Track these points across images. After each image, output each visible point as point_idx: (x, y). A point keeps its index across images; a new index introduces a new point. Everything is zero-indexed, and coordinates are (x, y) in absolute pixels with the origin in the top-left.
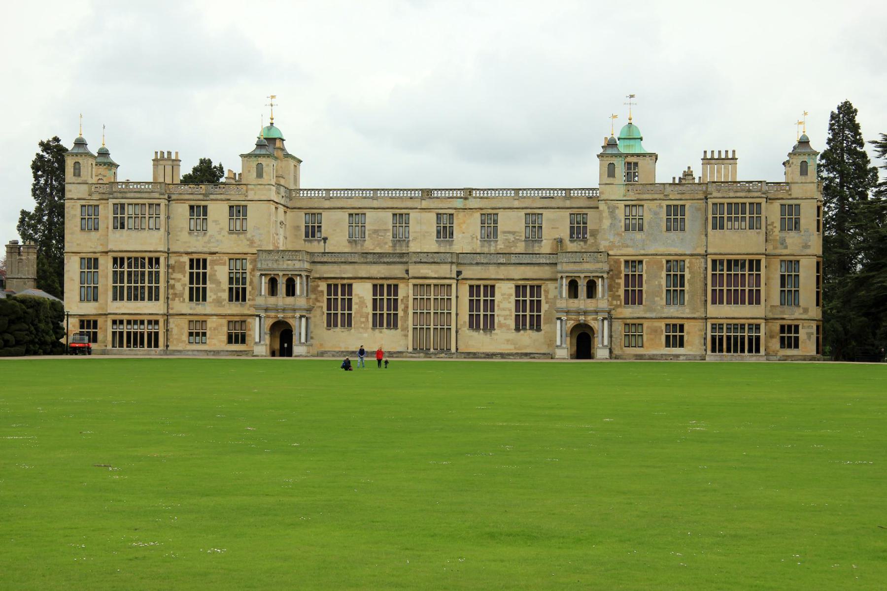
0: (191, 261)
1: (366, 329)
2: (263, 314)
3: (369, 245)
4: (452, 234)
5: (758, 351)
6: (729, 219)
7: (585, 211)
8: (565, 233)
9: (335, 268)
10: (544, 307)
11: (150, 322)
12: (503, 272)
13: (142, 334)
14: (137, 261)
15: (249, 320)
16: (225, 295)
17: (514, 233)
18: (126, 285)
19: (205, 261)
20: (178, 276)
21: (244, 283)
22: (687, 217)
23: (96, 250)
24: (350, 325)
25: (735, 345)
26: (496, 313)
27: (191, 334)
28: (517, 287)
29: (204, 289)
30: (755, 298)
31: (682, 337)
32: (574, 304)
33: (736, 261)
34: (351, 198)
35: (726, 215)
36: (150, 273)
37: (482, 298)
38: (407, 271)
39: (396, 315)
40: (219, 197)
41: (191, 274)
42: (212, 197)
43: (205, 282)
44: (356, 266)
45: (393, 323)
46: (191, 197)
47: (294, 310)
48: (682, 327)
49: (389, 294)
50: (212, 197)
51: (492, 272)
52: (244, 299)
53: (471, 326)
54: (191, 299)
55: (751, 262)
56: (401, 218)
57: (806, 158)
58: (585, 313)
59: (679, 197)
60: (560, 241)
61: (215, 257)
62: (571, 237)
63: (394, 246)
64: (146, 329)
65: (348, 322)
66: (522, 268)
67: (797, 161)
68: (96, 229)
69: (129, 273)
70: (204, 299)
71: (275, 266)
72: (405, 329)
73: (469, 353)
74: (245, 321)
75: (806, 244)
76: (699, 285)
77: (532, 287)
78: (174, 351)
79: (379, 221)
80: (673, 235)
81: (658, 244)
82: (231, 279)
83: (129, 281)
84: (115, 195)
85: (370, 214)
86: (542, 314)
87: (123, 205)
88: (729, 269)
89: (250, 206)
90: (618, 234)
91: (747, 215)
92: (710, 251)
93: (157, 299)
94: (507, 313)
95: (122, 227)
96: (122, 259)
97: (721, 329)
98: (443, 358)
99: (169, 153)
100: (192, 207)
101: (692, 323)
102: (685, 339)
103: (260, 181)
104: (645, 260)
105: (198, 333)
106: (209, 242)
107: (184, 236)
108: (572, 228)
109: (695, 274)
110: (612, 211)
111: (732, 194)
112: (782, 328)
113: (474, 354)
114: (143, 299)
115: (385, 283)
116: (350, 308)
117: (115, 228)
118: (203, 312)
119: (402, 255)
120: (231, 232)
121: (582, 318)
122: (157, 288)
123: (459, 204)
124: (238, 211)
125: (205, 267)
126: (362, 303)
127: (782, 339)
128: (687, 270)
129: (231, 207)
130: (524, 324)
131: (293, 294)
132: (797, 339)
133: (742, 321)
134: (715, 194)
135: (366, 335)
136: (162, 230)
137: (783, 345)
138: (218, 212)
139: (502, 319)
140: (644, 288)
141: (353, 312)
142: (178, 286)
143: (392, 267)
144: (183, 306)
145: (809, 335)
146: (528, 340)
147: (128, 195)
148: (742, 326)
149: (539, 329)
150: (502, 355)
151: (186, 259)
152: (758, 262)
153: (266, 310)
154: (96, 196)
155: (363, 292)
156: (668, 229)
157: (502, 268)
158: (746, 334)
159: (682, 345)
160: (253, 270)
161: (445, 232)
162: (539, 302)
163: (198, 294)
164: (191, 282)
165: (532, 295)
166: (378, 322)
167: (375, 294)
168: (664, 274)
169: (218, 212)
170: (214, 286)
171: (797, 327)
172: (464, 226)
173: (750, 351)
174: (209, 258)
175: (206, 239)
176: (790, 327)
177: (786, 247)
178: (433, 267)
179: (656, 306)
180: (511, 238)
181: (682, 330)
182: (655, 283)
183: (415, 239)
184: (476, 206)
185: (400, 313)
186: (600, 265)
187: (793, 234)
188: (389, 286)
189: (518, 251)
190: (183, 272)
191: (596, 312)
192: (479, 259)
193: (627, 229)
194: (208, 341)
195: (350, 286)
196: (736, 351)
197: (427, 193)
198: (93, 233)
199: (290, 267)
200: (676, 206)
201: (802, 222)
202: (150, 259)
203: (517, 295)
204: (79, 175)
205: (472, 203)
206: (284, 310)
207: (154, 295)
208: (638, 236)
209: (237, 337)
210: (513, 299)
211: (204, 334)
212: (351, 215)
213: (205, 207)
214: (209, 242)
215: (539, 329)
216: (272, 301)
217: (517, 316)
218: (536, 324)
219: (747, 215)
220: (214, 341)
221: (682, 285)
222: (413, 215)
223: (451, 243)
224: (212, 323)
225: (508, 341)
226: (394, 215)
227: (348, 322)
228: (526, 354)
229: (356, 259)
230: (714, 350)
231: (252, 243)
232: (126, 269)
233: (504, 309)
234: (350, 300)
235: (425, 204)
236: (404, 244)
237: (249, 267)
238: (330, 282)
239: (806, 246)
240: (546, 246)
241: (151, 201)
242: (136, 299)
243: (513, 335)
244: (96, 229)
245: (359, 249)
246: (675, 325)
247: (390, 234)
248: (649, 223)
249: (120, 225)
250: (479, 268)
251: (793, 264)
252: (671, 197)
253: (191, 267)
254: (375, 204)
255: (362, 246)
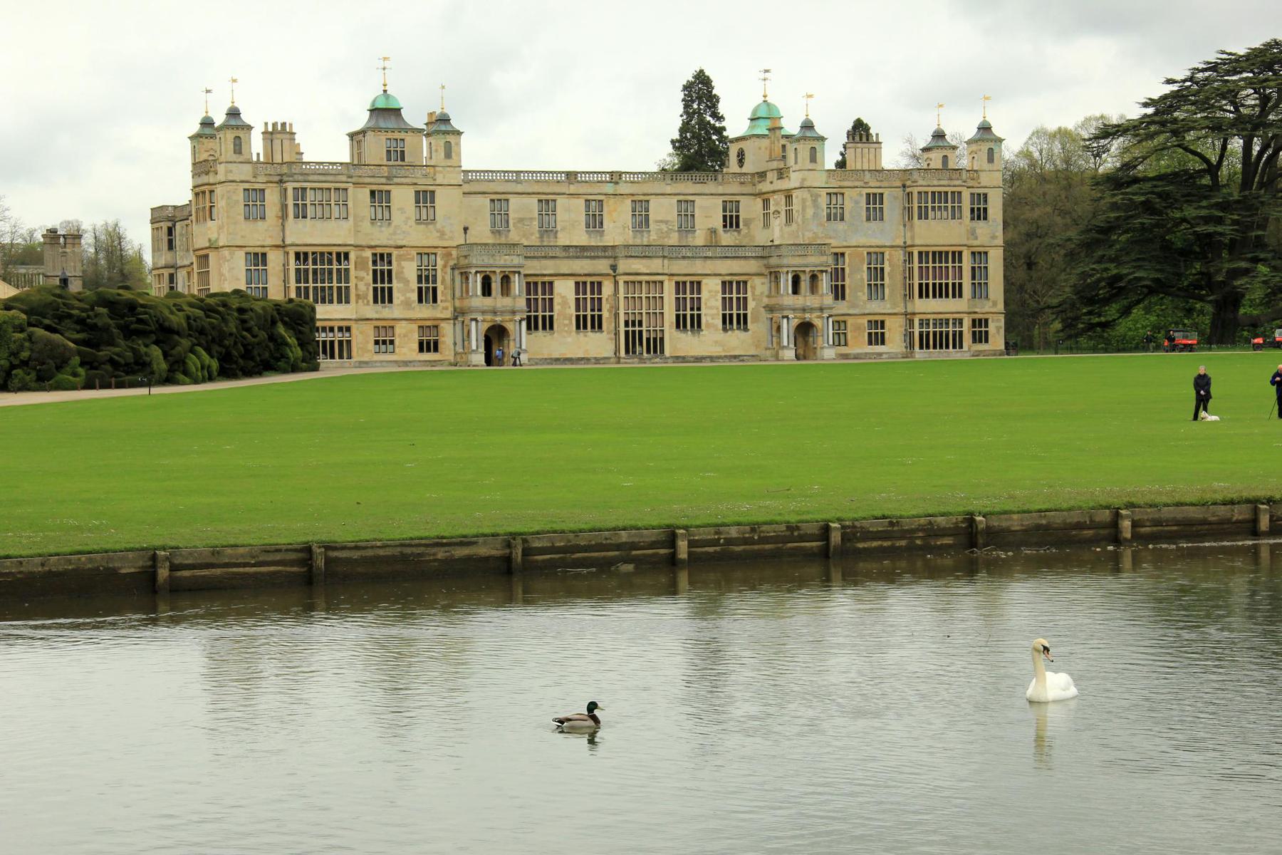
0: (374, 255)
1: (569, 332)
2: (480, 318)
3: (514, 236)
4: (602, 223)
5: (961, 347)
6: (933, 208)
7: (737, 198)
8: (718, 223)
9: (535, 263)
10: (751, 305)
11: (340, 329)
12: (710, 266)
13: (332, 343)
14: (321, 257)
15: (443, 325)
16: (415, 296)
17: (666, 222)
18: (311, 285)
19: (390, 255)
20: (362, 274)
21: (435, 281)
22: (885, 206)
23: (266, 243)
24: (551, 327)
25: (941, 341)
26: (703, 312)
27: (377, 342)
28: (724, 283)
29: (390, 289)
30: (957, 291)
31: (883, 334)
32: (799, 301)
33: (940, 253)
34: (493, 181)
35: (930, 205)
36: (338, 270)
37: (688, 296)
38: (614, 268)
39: (600, 317)
40: (403, 180)
41: (375, 272)
42: (396, 180)
43: (390, 281)
44: (558, 262)
45: (597, 324)
46: (372, 180)
47: (514, 312)
48: (883, 322)
49: (593, 293)
50: (396, 180)
51: (698, 267)
52: (435, 300)
53: (678, 326)
54: (375, 301)
55: (954, 253)
56: (547, 204)
57: (992, 145)
58: (812, 310)
59: (878, 184)
60: (713, 232)
61: (402, 251)
62: (725, 226)
63: (541, 237)
64: (338, 336)
65: (549, 324)
66: (729, 262)
67: (985, 147)
68: (263, 218)
69: (315, 271)
70: (390, 301)
71: (491, 262)
72: (617, 334)
73: (677, 357)
74: (436, 327)
75: (991, 234)
76: (899, 278)
77: (738, 283)
78: (360, 362)
79: (522, 208)
80: (873, 224)
81: (859, 235)
82: (420, 277)
83: (315, 281)
84: (296, 177)
85: (514, 200)
86: (749, 312)
87: (304, 189)
88: (934, 262)
89: (439, 192)
90: (821, 225)
91: (949, 205)
92: (917, 242)
93: (348, 302)
94: (714, 311)
95: (305, 217)
96: (306, 254)
97: (928, 324)
98: (657, 363)
99: (284, 125)
100: (372, 193)
101: (893, 319)
102: (886, 336)
103: (449, 162)
104: (847, 252)
105: (384, 342)
106: (395, 233)
107: (366, 225)
108: (725, 217)
109: (893, 265)
110: (815, 199)
111: (936, 183)
112: (974, 321)
113: (684, 358)
114: (331, 302)
115: (589, 280)
116: (551, 310)
117: (296, 217)
118: (391, 316)
119: (605, 248)
120: (419, 221)
121: (807, 315)
122: (347, 288)
123: (609, 188)
124: (425, 198)
125: (390, 263)
126: (565, 303)
127: (974, 333)
128: (887, 263)
129: (417, 193)
130: (731, 322)
131: (489, 294)
132: (987, 332)
133: (947, 316)
134: (921, 182)
135: (569, 340)
136: (351, 218)
137: (974, 341)
138: (403, 198)
139: (709, 318)
140: (847, 282)
141: (555, 314)
142: (362, 287)
143: (596, 262)
144: (372, 311)
145: (998, 328)
146: (737, 341)
147: (311, 178)
148: (947, 320)
149: (746, 329)
150: (712, 359)
151: (368, 254)
152: (960, 253)
153: (483, 312)
154: (260, 179)
155: (565, 291)
156: (868, 219)
157: (709, 262)
158: (951, 329)
159: (883, 343)
160: (445, 266)
161: (595, 222)
162: (745, 299)
163: (383, 296)
164: (375, 281)
165: (738, 292)
166: (581, 323)
167: (577, 293)
168: (865, 266)
169: (403, 198)
170: (401, 285)
171: (986, 321)
172: (615, 214)
173: (954, 347)
174: (395, 253)
175: (391, 230)
176: (980, 320)
177: (976, 238)
178: (644, 261)
179: (859, 303)
180: (664, 227)
181: (883, 327)
182: (856, 278)
183: (564, 229)
184: (627, 191)
185: (605, 314)
186: (824, 259)
187: (982, 223)
188: (592, 283)
189: (671, 242)
190: (364, 268)
191: (821, 309)
192: (684, 252)
193: (829, 219)
194: (397, 350)
195: (551, 283)
196: (941, 347)
197: (571, 176)
198: (260, 223)
199: (508, 263)
200: (875, 194)
201: (990, 212)
202: (338, 254)
203: (724, 292)
204: (240, 153)
205: (623, 188)
206: (502, 313)
207: (343, 297)
208: (840, 226)
209: (429, 345)
210: (720, 296)
211: (392, 342)
212: (492, 201)
213: (388, 192)
214: (395, 233)
215: (746, 329)
216: (488, 302)
217: (724, 316)
218: (743, 321)
219: (949, 205)
220: (405, 350)
221: (882, 279)
222: (561, 201)
223: (602, 234)
224: (400, 329)
225: (716, 342)
226: (540, 201)
227: (549, 324)
228: (735, 357)
229: (558, 253)
230: (921, 347)
231: (442, 234)
232: (311, 267)
233: (711, 308)
234: (551, 300)
235: (573, 189)
236: (552, 235)
237: (440, 262)
238: (530, 279)
239: (994, 237)
240: (699, 238)
241: (337, 185)
242: (323, 301)
243: (721, 335)
244: (263, 218)
245: (503, 240)
246: (876, 322)
247: (536, 223)
248: (851, 212)
249: (301, 213)
250: (685, 262)
251: (980, 255)
252: (872, 184)
253: (375, 263)
254: (519, 188)
255: (507, 237)
